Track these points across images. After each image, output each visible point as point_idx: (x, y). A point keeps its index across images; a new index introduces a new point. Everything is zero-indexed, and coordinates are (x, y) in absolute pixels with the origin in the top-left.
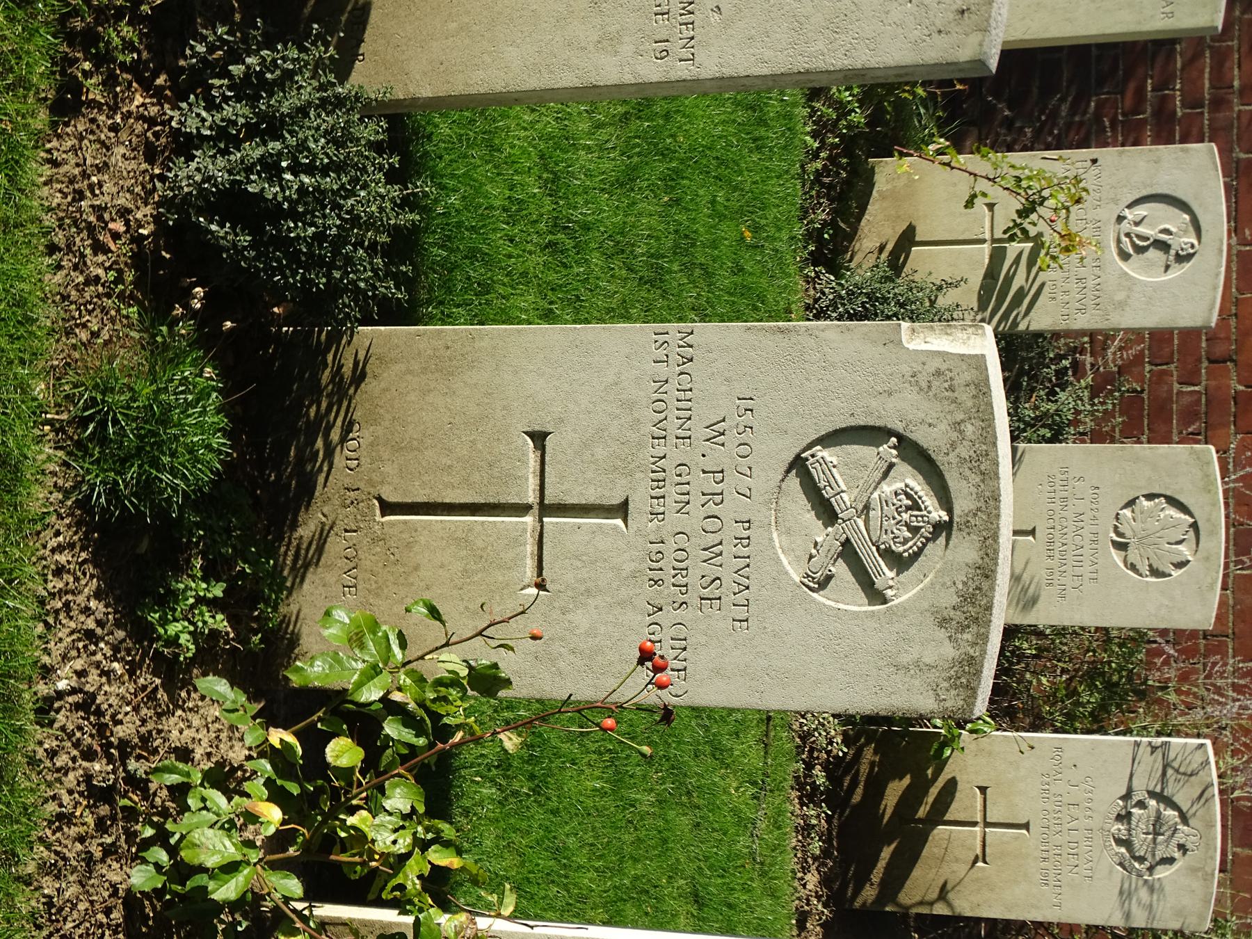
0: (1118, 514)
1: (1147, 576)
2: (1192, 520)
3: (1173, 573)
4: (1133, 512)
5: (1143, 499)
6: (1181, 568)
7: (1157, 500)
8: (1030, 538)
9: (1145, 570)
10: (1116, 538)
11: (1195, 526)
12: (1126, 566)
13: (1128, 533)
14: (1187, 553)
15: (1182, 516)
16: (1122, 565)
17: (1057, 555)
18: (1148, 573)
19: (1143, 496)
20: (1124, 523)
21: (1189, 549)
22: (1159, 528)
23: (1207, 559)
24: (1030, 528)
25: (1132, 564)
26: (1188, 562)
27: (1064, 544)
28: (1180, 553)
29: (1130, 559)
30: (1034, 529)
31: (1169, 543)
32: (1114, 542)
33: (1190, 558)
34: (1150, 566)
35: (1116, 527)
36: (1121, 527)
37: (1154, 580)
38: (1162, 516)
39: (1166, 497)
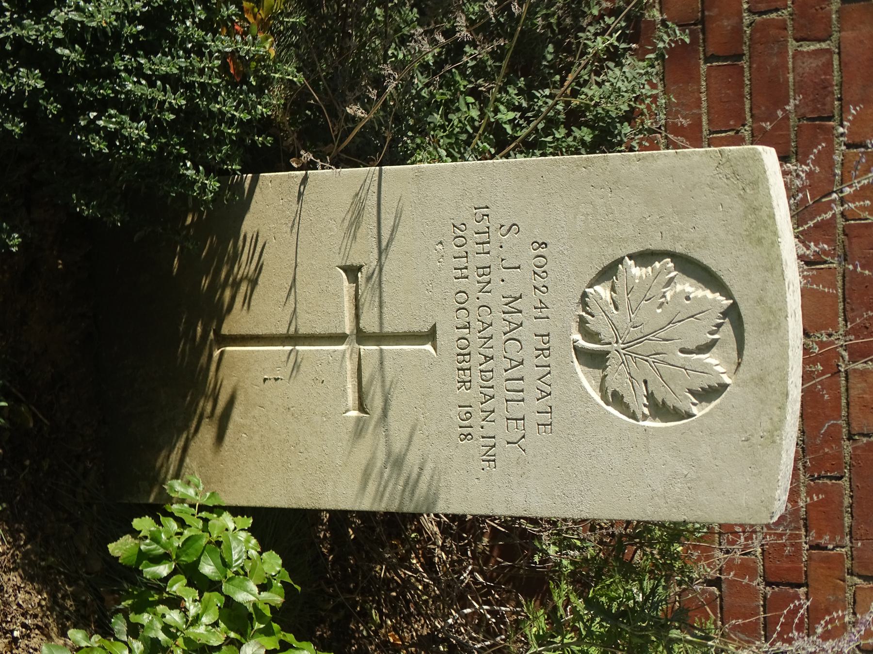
0: (585, 295)
1: (645, 417)
2: (731, 301)
3: (694, 410)
4: (613, 289)
5: (631, 263)
6: (709, 401)
7: (657, 265)
8: (428, 347)
9: (640, 405)
10: (583, 343)
11: (733, 314)
12: (604, 397)
13: (606, 333)
14: (720, 369)
15: (708, 294)
16: (597, 397)
17: (477, 380)
18: (646, 411)
19: (631, 257)
20: (600, 315)
21: (725, 360)
22: (663, 321)
23: (760, 381)
24: (426, 328)
25: (615, 394)
26: (724, 387)
27: (488, 358)
28: (706, 370)
29: (612, 384)
30: (434, 329)
31: (683, 351)
32: (579, 352)
33: (727, 380)
34: (650, 396)
35: (582, 321)
36: (593, 324)
37: (658, 424)
38: (669, 295)
39: (673, 255)
